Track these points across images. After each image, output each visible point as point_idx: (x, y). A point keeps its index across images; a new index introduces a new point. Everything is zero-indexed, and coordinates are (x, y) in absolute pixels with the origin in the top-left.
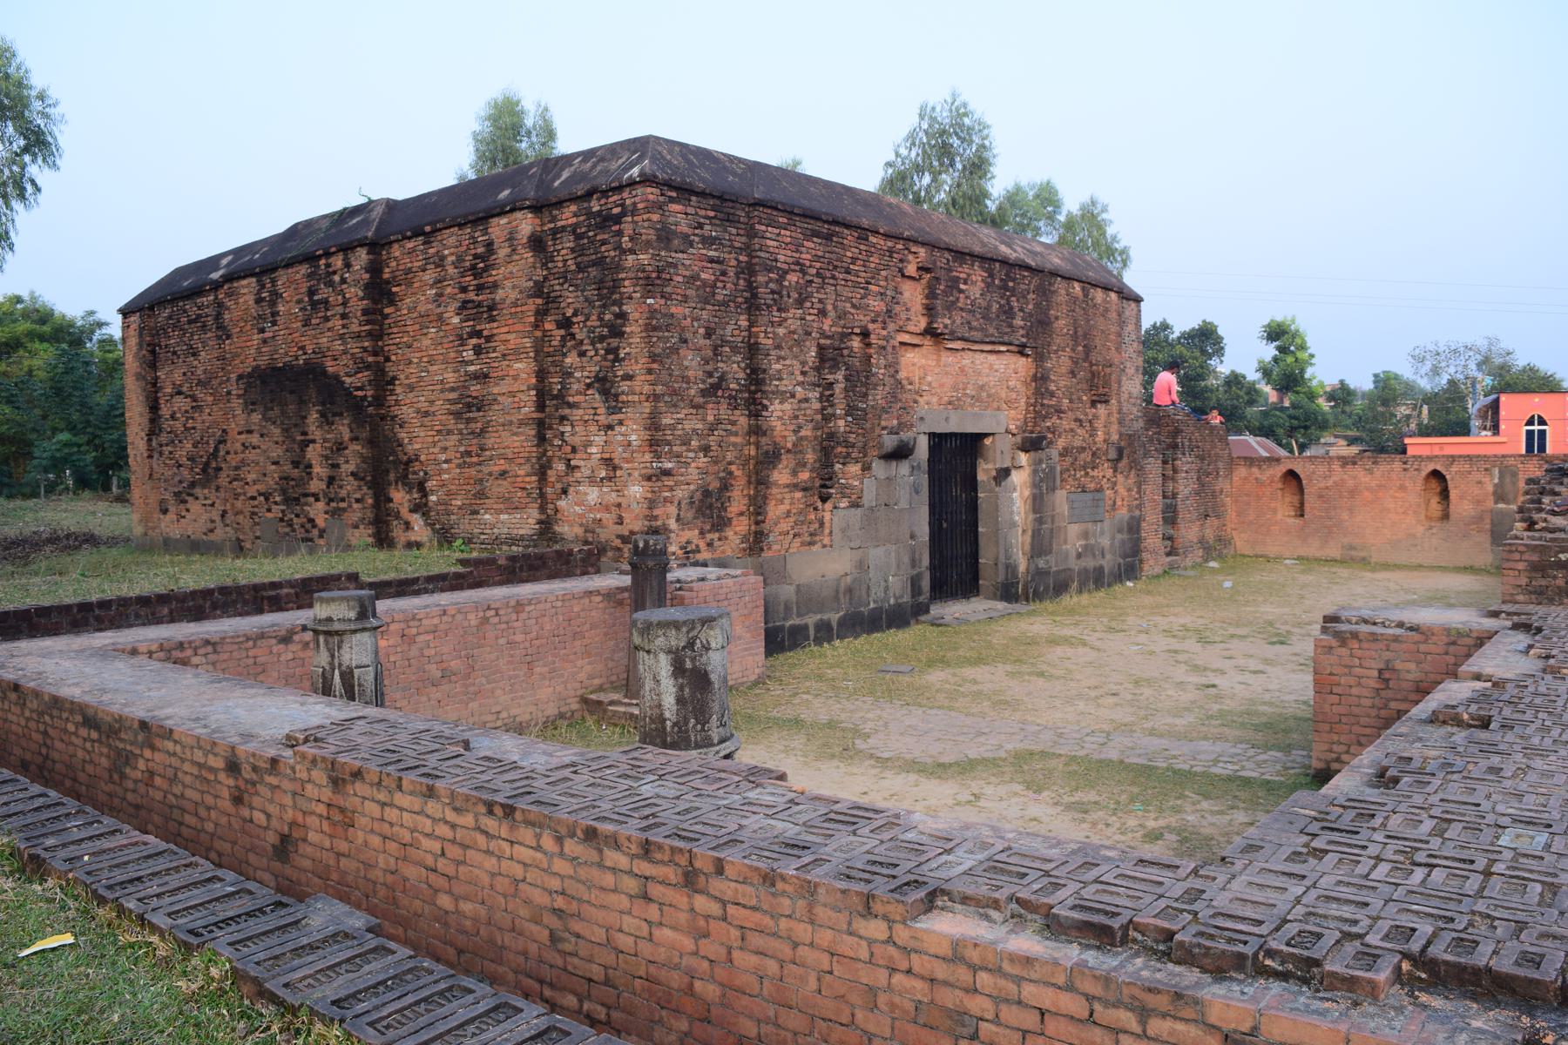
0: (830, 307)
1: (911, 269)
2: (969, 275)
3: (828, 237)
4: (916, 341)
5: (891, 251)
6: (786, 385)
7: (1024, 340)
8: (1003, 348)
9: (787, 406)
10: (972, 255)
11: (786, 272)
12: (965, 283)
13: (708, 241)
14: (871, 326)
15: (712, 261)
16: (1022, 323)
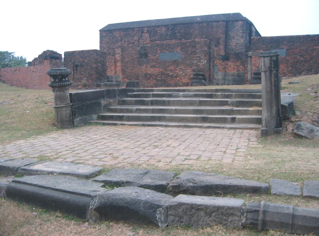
0: (126, 41)
1: (145, 31)
2: (160, 30)
3: (126, 31)
4: (150, 42)
5: (139, 30)
6: (119, 52)
7: (180, 38)
8: (174, 40)
9: (119, 55)
10: (161, 26)
11: (118, 38)
12: (159, 31)
13: (108, 36)
14: (134, 42)
15: (109, 38)
16: (179, 35)
